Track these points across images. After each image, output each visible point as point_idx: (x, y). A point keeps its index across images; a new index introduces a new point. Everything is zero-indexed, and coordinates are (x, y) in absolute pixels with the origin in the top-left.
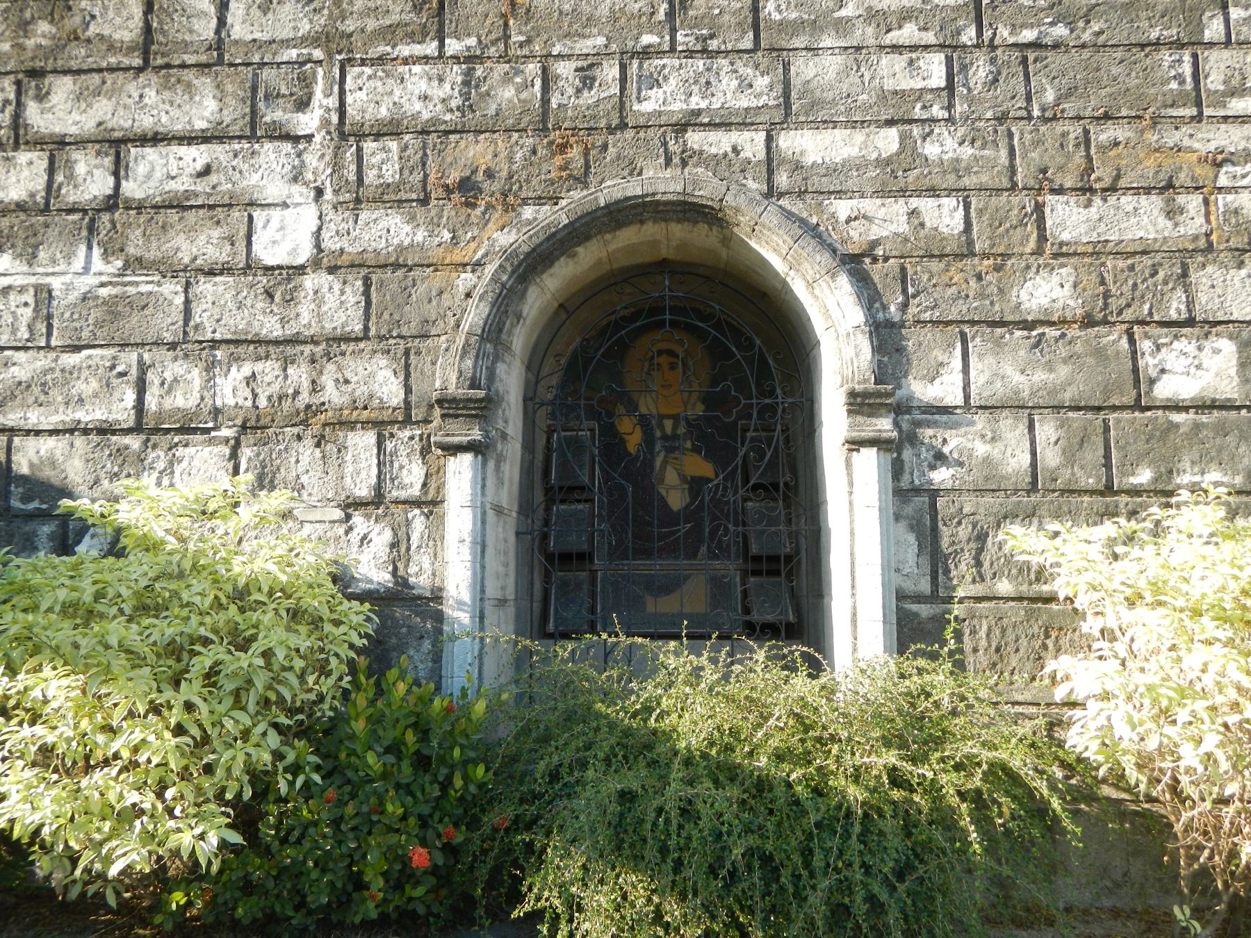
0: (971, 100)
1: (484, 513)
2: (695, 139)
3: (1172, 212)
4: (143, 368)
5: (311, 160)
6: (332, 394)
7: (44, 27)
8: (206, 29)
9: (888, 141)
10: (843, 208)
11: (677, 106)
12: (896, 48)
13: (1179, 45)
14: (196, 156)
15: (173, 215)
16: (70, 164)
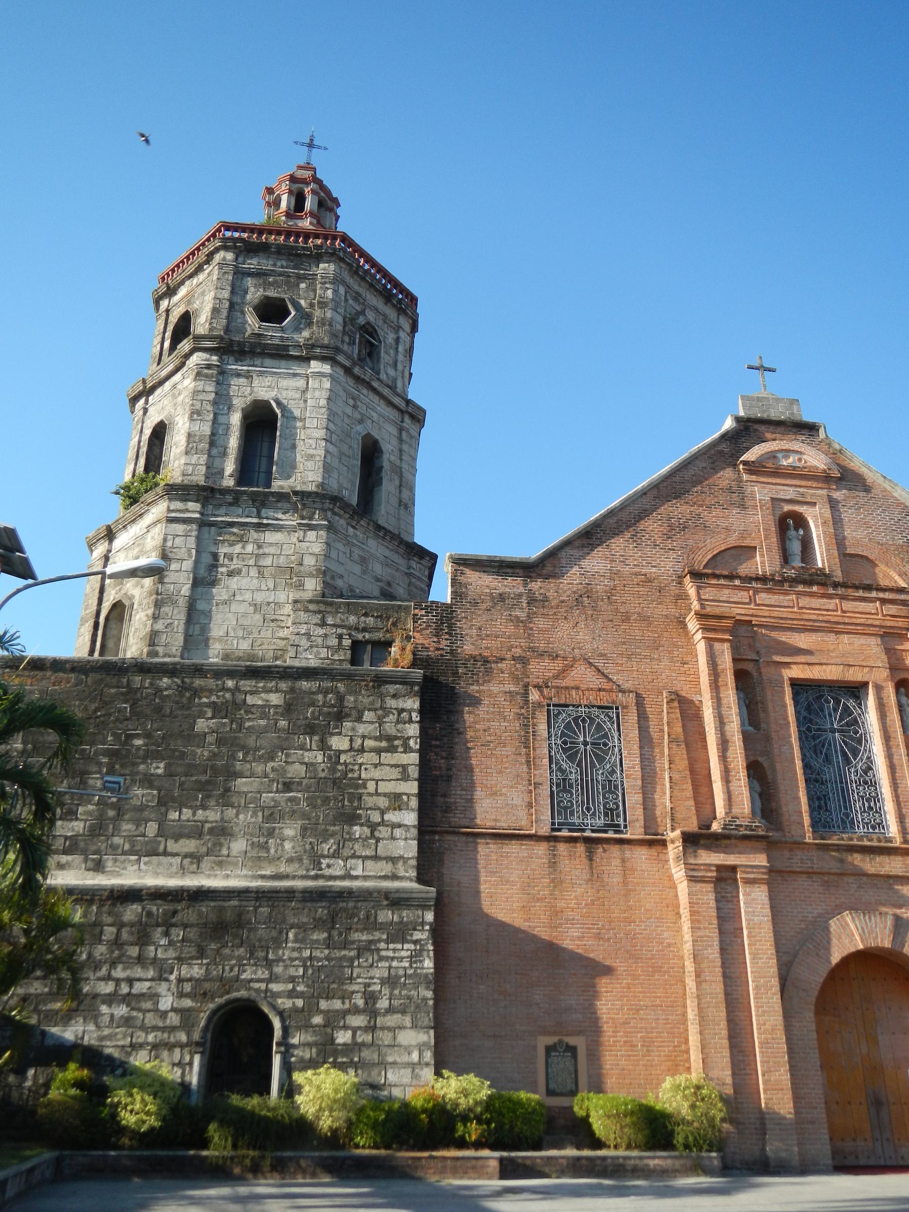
0: (308, 978)
1: (201, 1066)
2: (252, 984)
3: (343, 1003)
4: (132, 1033)
5: (172, 986)
6: (172, 1039)
7: (117, 952)
8: (152, 955)
9: (290, 986)
10: (280, 1001)
11: (249, 977)
12: (294, 966)
13: (349, 967)
14: (148, 984)
15: (141, 998)
16: (120, 986)
